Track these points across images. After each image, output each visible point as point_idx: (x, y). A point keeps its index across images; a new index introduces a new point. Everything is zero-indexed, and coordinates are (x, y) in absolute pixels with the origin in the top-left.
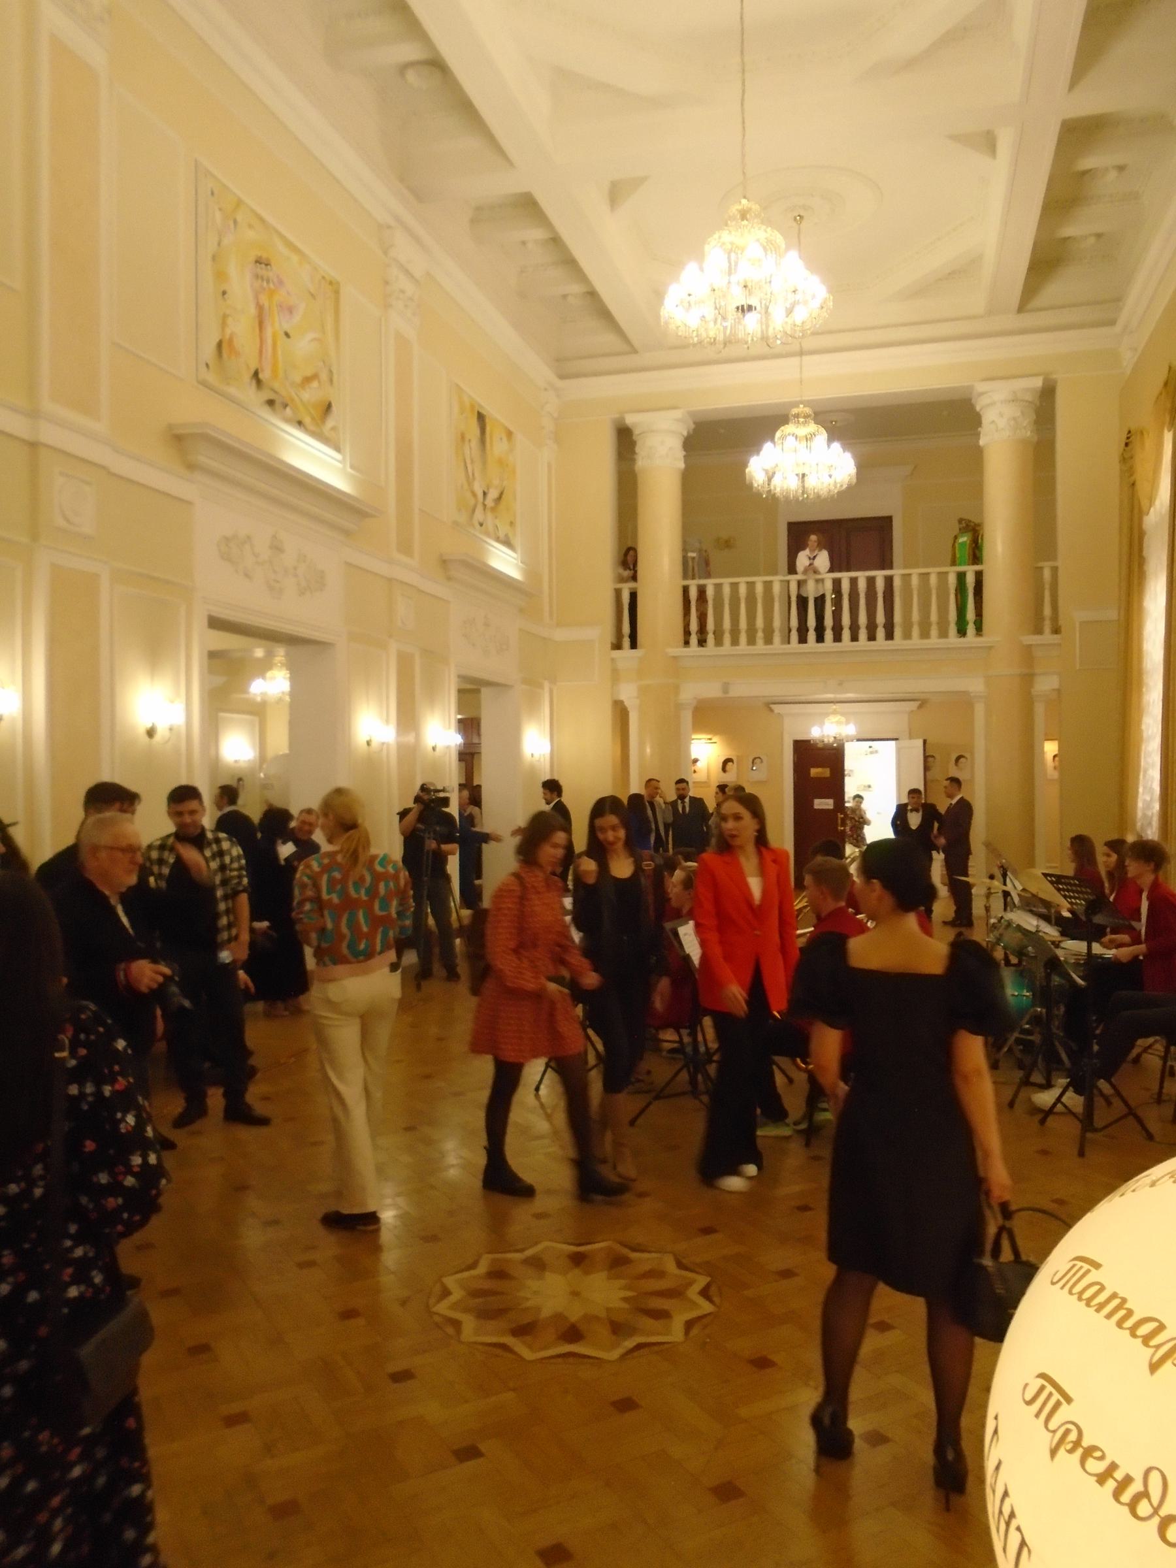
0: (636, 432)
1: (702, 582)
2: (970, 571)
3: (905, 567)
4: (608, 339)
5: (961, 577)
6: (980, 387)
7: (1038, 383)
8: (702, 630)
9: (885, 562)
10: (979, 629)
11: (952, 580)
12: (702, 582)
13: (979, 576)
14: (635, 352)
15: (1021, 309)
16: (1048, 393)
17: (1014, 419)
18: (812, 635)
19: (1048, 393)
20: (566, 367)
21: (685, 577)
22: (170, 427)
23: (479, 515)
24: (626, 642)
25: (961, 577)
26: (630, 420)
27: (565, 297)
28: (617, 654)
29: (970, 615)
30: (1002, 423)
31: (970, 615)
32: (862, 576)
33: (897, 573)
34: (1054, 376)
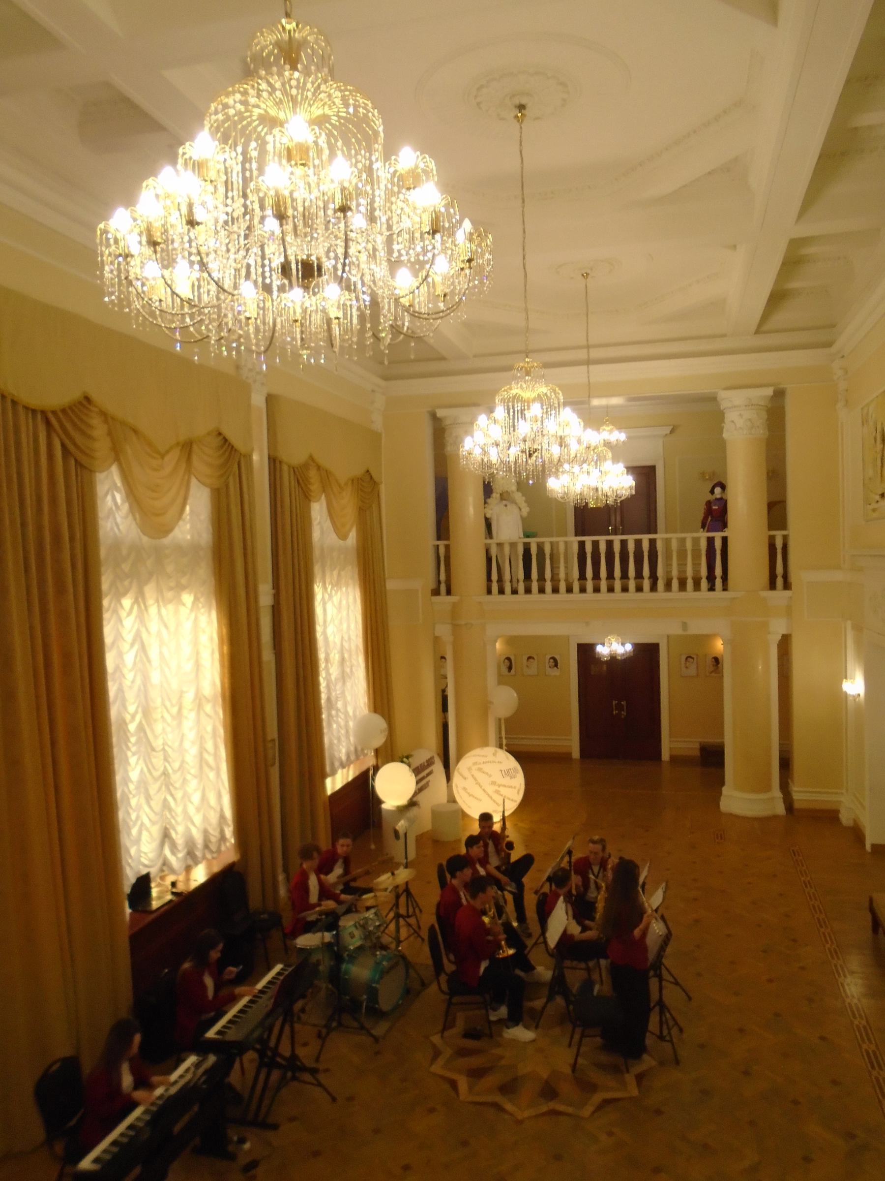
0: (448, 422)
3: (667, 532)
7: (770, 392)
11: (703, 544)
13: (725, 540)
15: (757, 332)
16: (779, 394)
17: (750, 420)
19: (779, 394)
26: (440, 413)
29: (718, 571)
30: (740, 423)
31: (718, 571)
33: (659, 537)
34: (782, 386)
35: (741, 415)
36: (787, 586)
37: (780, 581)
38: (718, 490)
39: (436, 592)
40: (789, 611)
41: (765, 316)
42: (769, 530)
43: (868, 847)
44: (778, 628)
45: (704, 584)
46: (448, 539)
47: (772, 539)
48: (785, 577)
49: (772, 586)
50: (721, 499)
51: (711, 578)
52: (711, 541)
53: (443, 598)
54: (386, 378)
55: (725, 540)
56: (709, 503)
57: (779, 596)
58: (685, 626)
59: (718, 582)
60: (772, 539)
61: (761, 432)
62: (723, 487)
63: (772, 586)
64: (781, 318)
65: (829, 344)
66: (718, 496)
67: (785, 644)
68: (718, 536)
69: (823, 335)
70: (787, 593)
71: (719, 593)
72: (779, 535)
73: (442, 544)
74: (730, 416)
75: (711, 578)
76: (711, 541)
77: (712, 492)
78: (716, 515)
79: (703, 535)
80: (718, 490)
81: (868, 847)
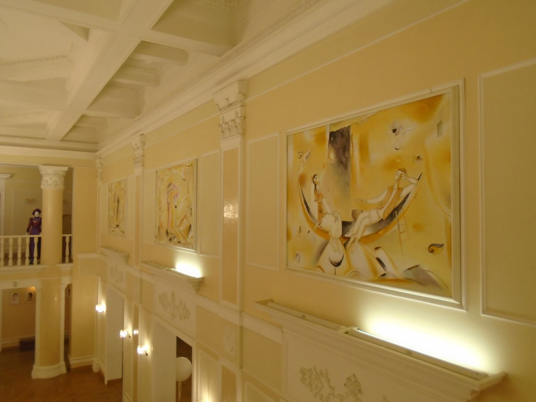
7: (66, 169)
10: (39, 263)
11: (28, 241)
13: (40, 239)
17: (55, 181)
29: (35, 254)
30: (50, 182)
31: (35, 254)
35: (51, 179)
36: (71, 261)
37: (67, 259)
38: (37, 213)
40: (71, 273)
42: (63, 233)
43: (106, 383)
44: (66, 281)
45: (27, 261)
47: (64, 238)
48: (70, 255)
49: (63, 261)
50: (38, 217)
51: (31, 258)
52: (32, 240)
55: (40, 239)
56: (31, 219)
57: (67, 266)
58: (15, 284)
59: (35, 260)
60: (64, 238)
61: (61, 187)
62: (39, 211)
63: (63, 261)
65: (95, 151)
66: (37, 216)
67: (69, 290)
68: (36, 237)
69: (93, 146)
70: (71, 265)
71: (35, 266)
72: (67, 236)
74: (45, 178)
75: (31, 258)
76: (32, 240)
77: (34, 214)
78: (35, 226)
79: (28, 237)
80: (37, 213)
81: (106, 383)
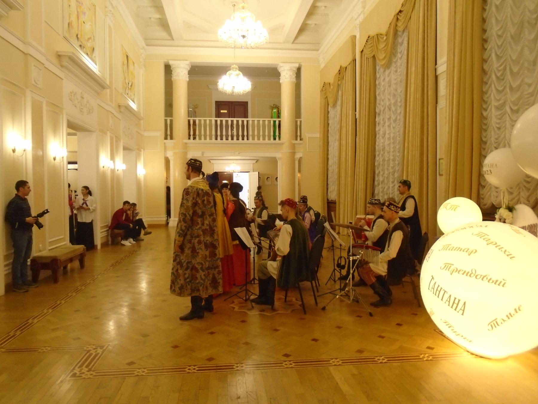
0: (172, 67)
1: (195, 119)
2: (277, 120)
4: (164, 34)
5: (275, 122)
6: (281, 65)
7: (297, 65)
8: (194, 134)
9: (246, 116)
12: (195, 119)
13: (280, 122)
14: (173, 40)
15: (293, 43)
16: (299, 70)
18: (219, 138)
19: (299, 70)
20: (149, 42)
21: (189, 117)
22: (57, 52)
23: (127, 91)
24: (169, 137)
25: (275, 122)
27: (150, 18)
28: (166, 141)
29: (277, 134)
30: (287, 76)
31: (277, 134)
32: (235, 120)
39: (166, 138)
41: (296, 38)
46: (172, 116)
47: (296, 122)
48: (300, 136)
53: (169, 141)
54: (147, 45)
64: (302, 38)
65: (318, 50)
72: (299, 120)
73: (169, 119)
